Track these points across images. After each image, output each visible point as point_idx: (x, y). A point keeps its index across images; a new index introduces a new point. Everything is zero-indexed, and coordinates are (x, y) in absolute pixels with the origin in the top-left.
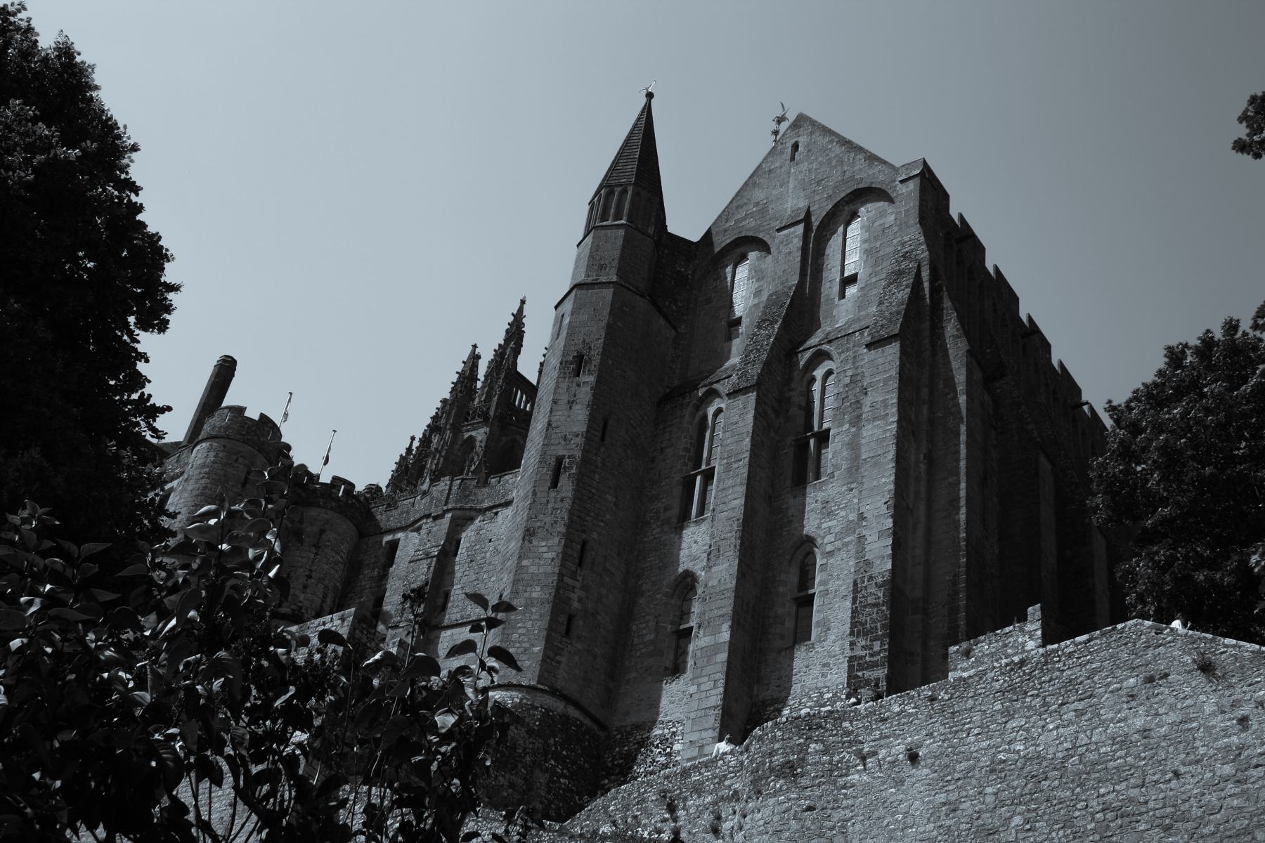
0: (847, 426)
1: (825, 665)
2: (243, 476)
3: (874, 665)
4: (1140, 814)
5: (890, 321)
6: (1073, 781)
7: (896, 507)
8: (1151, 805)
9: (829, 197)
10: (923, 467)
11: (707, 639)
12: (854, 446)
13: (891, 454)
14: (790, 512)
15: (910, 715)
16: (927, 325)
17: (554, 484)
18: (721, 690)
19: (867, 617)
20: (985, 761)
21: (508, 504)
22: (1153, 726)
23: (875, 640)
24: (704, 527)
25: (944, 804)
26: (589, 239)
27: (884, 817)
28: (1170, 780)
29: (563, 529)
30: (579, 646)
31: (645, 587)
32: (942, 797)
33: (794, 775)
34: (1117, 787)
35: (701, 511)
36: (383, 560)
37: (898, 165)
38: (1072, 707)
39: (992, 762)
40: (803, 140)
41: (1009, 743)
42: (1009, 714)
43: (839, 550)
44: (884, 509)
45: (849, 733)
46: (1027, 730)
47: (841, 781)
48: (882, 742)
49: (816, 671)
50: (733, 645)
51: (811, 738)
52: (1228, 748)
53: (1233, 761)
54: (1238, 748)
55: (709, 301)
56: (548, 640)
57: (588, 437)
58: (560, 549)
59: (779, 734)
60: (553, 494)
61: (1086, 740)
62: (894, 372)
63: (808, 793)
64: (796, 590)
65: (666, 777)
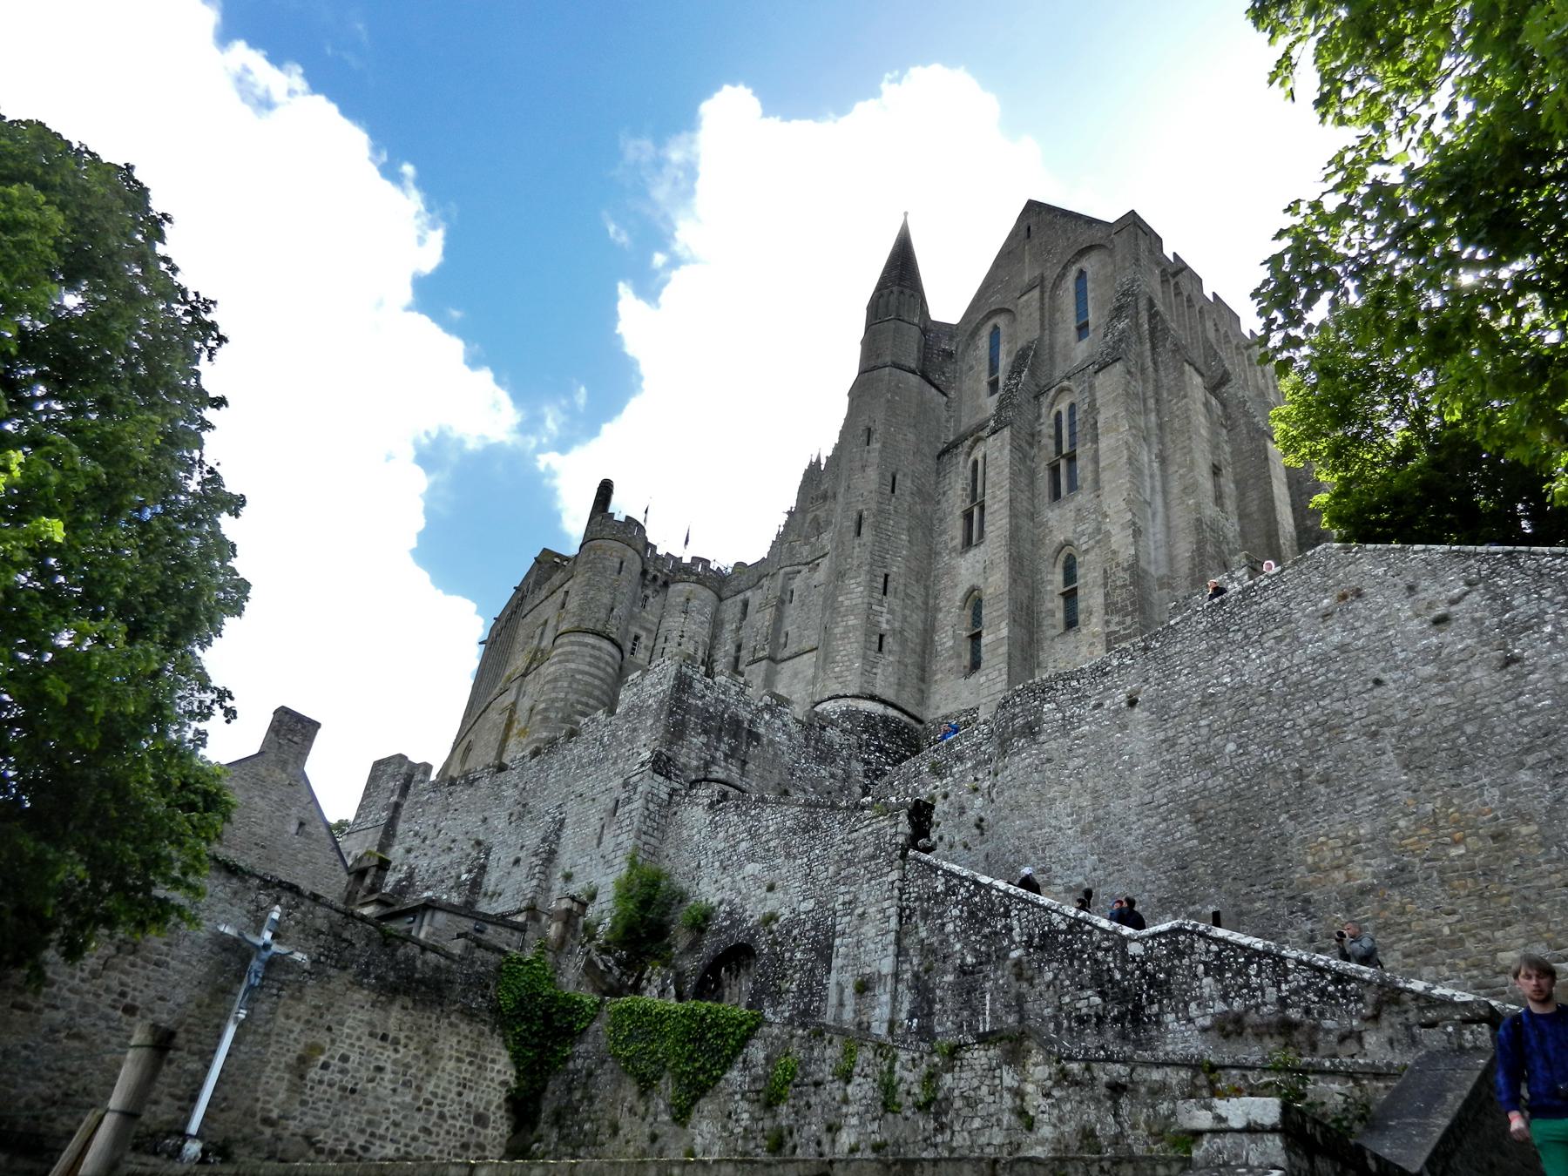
1: (1092, 644)
2: (618, 566)
6: (1279, 704)
9: (1059, 262)
10: (1155, 465)
11: (990, 637)
14: (1050, 523)
15: (1128, 666)
16: (1148, 346)
17: (859, 534)
18: (1005, 677)
19: (1119, 597)
20: (1197, 697)
21: (823, 556)
23: (1126, 615)
25: (1164, 741)
28: (1371, 689)
29: (866, 568)
30: (891, 658)
31: (942, 604)
32: (1161, 736)
33: (1033, 734)
34: (1321, 703)
38: (1271, 635)
39: (1203, 697)
40: (1033, 220)
41: (1217, 678)
43: (1093, 547)
44: (1123, 505)
45: (1078, 690)
46: (1232, 663)
47: (1073, 734)
49: (1084, 650)
50: (1011, 640)
52: (1426, 649)
53: (1433, 660)
55: (971, 368)
56: (864, 657)
60: (857, 542)
63: (1046, 746)
64: (1061, 586)
65: (935, 751)
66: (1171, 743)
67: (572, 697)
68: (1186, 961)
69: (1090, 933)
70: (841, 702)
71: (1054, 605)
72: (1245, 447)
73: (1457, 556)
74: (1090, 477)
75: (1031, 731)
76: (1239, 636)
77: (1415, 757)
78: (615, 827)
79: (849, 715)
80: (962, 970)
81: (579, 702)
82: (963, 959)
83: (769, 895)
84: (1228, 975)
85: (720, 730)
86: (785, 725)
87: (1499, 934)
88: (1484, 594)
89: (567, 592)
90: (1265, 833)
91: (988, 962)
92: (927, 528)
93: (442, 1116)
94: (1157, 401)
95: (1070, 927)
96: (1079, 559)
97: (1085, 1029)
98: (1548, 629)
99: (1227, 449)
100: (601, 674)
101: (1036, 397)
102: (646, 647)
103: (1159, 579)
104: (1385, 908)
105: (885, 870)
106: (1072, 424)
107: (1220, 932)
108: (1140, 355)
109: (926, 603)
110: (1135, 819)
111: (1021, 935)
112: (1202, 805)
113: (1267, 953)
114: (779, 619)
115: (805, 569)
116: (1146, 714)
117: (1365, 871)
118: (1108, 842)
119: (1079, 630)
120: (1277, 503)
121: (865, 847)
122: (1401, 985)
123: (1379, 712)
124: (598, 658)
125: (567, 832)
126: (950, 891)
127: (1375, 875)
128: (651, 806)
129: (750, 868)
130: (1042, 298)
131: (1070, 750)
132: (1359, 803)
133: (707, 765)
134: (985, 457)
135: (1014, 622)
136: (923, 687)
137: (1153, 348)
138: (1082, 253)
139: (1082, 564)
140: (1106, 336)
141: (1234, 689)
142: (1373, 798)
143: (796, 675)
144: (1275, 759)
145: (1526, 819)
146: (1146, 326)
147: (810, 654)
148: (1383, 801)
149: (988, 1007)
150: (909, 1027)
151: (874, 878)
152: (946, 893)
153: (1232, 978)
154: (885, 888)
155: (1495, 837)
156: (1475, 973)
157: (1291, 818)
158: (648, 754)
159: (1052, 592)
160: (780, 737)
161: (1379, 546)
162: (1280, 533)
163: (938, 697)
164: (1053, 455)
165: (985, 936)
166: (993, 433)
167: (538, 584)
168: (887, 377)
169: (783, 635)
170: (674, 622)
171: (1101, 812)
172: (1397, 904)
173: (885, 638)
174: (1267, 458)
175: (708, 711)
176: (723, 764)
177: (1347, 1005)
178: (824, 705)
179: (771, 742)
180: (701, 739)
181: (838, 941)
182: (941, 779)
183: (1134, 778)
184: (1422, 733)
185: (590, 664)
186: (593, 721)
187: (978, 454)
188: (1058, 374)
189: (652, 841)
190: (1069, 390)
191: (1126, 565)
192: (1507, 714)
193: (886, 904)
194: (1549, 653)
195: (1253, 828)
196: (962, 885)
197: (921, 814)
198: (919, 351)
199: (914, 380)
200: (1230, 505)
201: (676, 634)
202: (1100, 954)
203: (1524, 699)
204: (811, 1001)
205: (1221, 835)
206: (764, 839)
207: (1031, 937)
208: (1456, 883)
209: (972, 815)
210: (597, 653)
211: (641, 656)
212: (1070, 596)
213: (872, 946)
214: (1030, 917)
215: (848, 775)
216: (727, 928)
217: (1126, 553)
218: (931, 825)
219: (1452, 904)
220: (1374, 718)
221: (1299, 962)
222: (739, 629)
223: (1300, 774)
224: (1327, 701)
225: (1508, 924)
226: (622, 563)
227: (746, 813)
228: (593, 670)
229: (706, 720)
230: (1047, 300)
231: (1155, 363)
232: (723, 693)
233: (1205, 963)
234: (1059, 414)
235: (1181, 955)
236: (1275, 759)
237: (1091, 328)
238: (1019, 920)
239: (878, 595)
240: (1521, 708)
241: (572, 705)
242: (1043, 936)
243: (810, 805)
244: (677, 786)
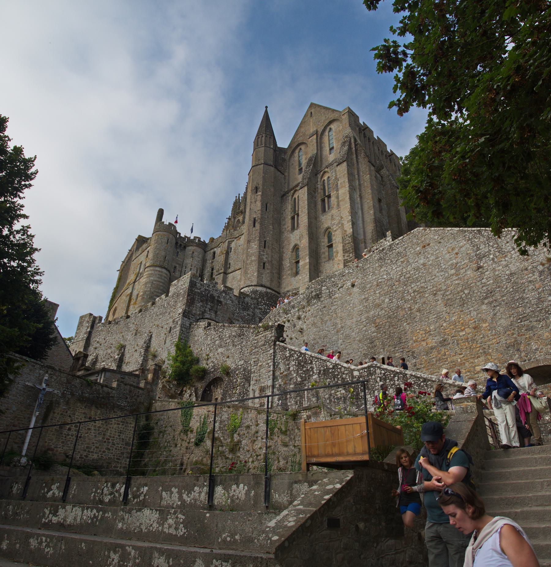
0: (335, 192)
1: (338, 264)
4: (426, 291)
5: (343, 157)
7: (351, 212)
8: (429, 288)
9: (323, 125)
11: (302, 262)
12: (338, 197)
13: (348, 197)
14: (322, 221)
15: (351, 273)
16: (355, 156)
17: (254, 226)
18: (308, 276)
19: (348, 247)
20: (375, 283)
21: (242, 234)
22: (427, 262)
25: (364, 299)
27: (347, 306)
28: (434, 279)
29: (258, 239)
30: (268, 271)
32: (363, 297)
33: (319, 298)
34: (417, 284)
36: (212, 257)
37: (341, 111)
38: (400, 261)
39: (377, 283)
40: (313, 111)
41: (382, 276)
42: (381, 266)
43: (338, 229)
47: (333, 297)
48: (344, 283)
50: (310, 264)
51: (322, 285)
52: (452, 265)
53: (454, 268)
54: (456, 264)
55: (292, 164)
56: (258, 271)
57: (262, 210)
58: (258, 244)
59: (313, 286)
60: (254, 229)
61: (405, 271)
62: (346, 172)
66: (367, 299)
67: (152, 290)
68: (373, 377)
69: (340, 368)
70: (251, 287)
72: (390, 192)
73: (461, 232)
74: (336, 204)
75: (318, 297)
76: (389, 261)
77: (449, 302)
78: (170, 337)
81: (155, 292)
82: (297, 380)
83: (227, 359)
84: (388, 381)
85: (207, 300)
86: (231, 297)
87: (476, 361)
88: (471, 245)
90: (399, 329)
91: (305, 380)
95: (334, 366)
96: (333, 234)
97: (339, 402)
98: (492, 256)
100: (163, 281)
101: (316, 175)
102: (179, 271)
104: (439, 353)
105: (269, 349)
107: (385, 366)
109: (280, 250)
110: (355, 326)
111: (317, 370)
112: (378, 321)
113: (401, 373)
116: (358, 289)
117: (432, 342)
118: (346, 335)
119: (334, 259)
121: (261, 341)
122: (445, 382)
123: (436, 287)
124: (161, 275)
125: (153, 339)
126: (291, 356)
127: (436, 342)
128: (183, 329)
129: (220, 350)
131: (332, 303)
132: (430, 318)
134: (298, 197)
135: (311, 257)
136: (280, 281)
137: (357, 157)
138: (331, 122)
139: (334, 235)
140: (340, 152)
141: (388, 280)
142: (435, 316)
143: (234, 278)
144: (402, 304)
145: (485, 321)
146: (354, 149)
147: (238, 271)
148: (439, 318)
149: (306, 396)
150: (278, 404)
151: (265, 352)
152: (290, 357)
153: (389, 382)
154: (269, 356)
155: (474, 328)
156: (468, 374)
157: (408, 324)
158: (181, 310)
159: (324, 245)
160: (229, 302)
161: (436, 228)
162: (402, 222)
163: (285, 284)
164: (323, 196)
165: (304, 371)
166: (301, 188)
167: (137, 249)
168: (262, 168)
169: (228, 264)
170: (189, 261)
172: (443, 352)
173: (265, 264)
175: (202, 294)
176: (209, 312)
177: (427, 389)
179: (226, 304)
180: (200, 304)
181: (252, 375)
182: (287, 315)
183: (354, 312)
184: (450, 294)
185: (158, 278)
186: (161, 298)
187: (296, 196)
188: (324, 166)
190: (327, 172)
191: (349, 235)
192: (478, 286)
193: (269, 361)
194: (492, 265)
195: (395, 328)
196: (295, 353)
197: (280, 329)
198: (273, 158)
199: (272, 169)
200: (384, 212)
202: (344, 376)
203: (483, 281)
205: (384, 331)
206: (224, 340)
207: (320, 371)
208: (462, 344)
209: (298, 327)
210: (160, 273)
211: (177, 274)
212: (330, 246)
213: (265, 376)
214: (320, 364)
215: (254, 314)
216: (213, 372)
218: (284, 331)
219: (461, 351)
220: (435, 289)
221: (411, 375)
222: (212, 262)
223: (410, 309)
224: (419, 283)
225: (479, 357)
226: (168, 240)
227: (217, 330)
228: (159, 280)
229: (201, 297)
230: (319, 139)
232: (208, 287)
233: (380, 377)
234: (324, 180)
235: (371, 374)
236: (402, 304)
237: (335, 149)
238: (316, 365)
240: (483, 284)
241: (153, 293)
242: (324, 370)
243: (241, 327)
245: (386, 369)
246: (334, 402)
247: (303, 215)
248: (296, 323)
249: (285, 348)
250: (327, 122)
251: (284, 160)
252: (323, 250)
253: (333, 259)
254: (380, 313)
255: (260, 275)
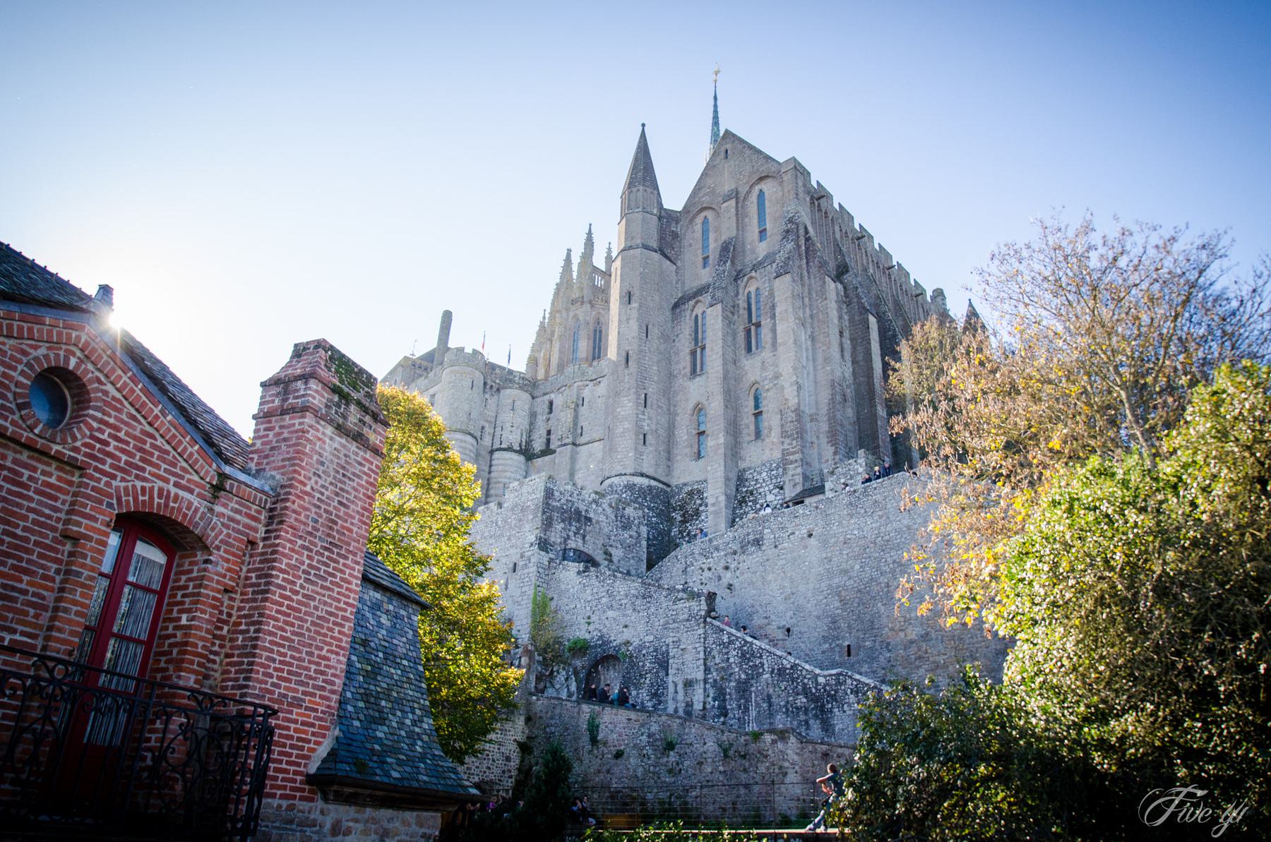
3: (793, 453)
9: (747, 182)
10: (809, 342)
16: (805, 261)
19: (790, 427)
20: (842, 539)
24: (704, 377)
26: (624, 220)
29: (634, 390)
32: (824, 555)
35: (702, 370)
36: (547, 410)
37: (781, 161)
42: (851, 516)
49: (767, 452)
55: (690, 245)
60: (626, 372)
62: (789, 294)
71: (748, 420)
72: (857, 318)
74: (770, 341)
75: (758, 543)
79: (630, 487)
80: (739, 681)
83: (625, 630)
89: (433, 396)
92: (667, 360)
93: (494, 761)
94: (810, 299)
99: (846, 317)
101: (736, 280)
103: (811, 415)
106: (758, 302)
108: (800, 267)
109: (669, 410)
114: (576, 417)
115: (591, 384)
120: (873, 356)
126: (731, 642)
128: (540, 570)
129: (610, 614)
130: (737, 208)
133: (565, 540)
137: (807, 263)
138: (761, 179)
143: (590, 455)
146: (803, 248)
160: (602, 518)
170: (507, 417)
171: (794, 590)
174: (868, 327)
178: (613, 479)
179: (598, 522)
181: (671, 661)
189: (542, 589)
193: (697, 645)
199: (657, 256)
201: (508, 425)
204: (658, 689)
207: (773, 670)
209: (725, 581)
210: (464, 444)
212: (758, 415)
216: (600, 646)
217: (793, 401)
231: (808, 273)
235: (841, 684)
239: (642, 408)
242: (779, 670)
244: (552, 556)
245: (859, 681)
246: (793, 712)
247: (714, 357)
248: (722, 575)
249: (722, 630)
250: (756, 177)
251: (675, 236)
252: (746, 421)
253: (763, 440)
254: (847, 584)
255: (639, 454)
